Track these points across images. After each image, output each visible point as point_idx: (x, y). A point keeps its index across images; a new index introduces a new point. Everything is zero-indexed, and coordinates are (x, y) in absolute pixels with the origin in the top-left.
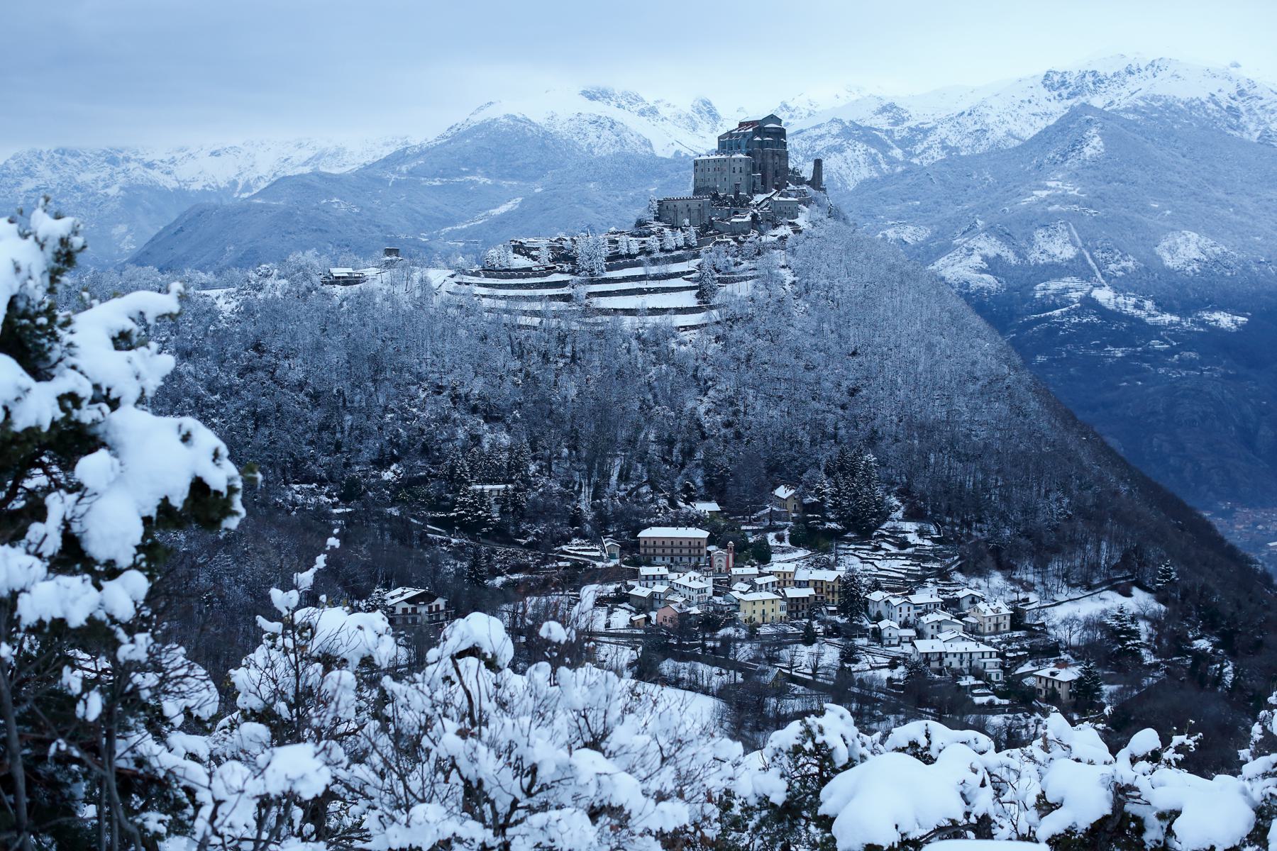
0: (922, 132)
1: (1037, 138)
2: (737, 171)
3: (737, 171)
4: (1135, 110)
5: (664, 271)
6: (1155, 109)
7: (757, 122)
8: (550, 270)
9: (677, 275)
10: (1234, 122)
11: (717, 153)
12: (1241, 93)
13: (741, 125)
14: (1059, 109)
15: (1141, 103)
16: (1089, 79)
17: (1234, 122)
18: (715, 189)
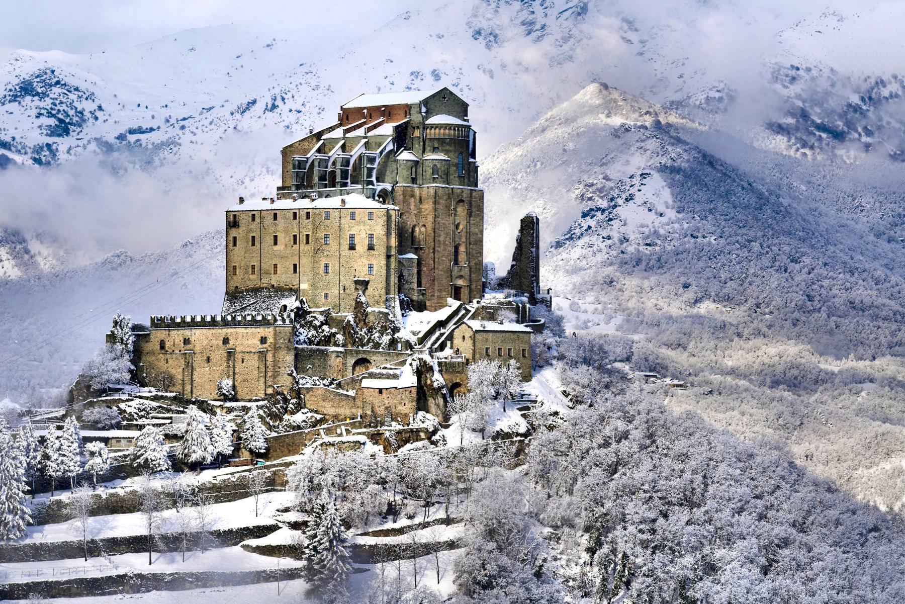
2: (361, 247)
3: (361, 247)
11: (283, 191)
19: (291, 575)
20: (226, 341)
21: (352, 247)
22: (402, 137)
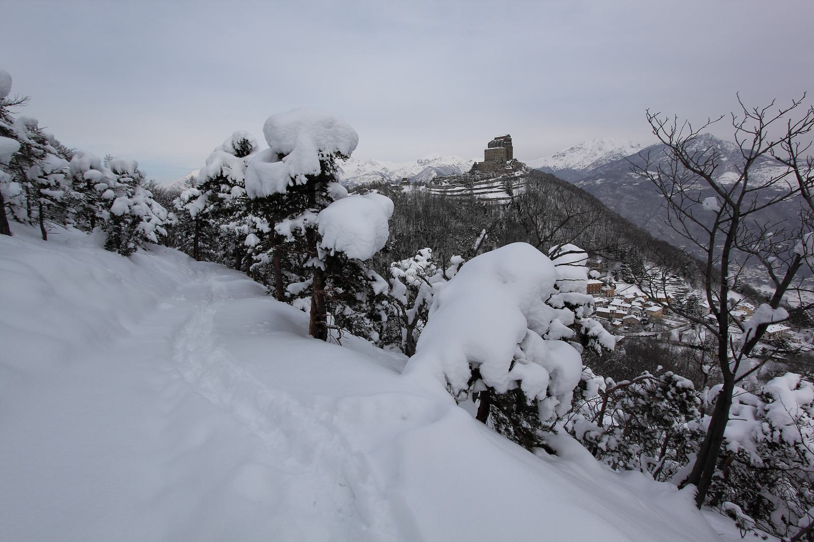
0: (392, 173)
1: (420, 174)
4: (439, 167)
8: (454, 187)
14: (421, 169)
16: (427, 161)
22: (505, 140)
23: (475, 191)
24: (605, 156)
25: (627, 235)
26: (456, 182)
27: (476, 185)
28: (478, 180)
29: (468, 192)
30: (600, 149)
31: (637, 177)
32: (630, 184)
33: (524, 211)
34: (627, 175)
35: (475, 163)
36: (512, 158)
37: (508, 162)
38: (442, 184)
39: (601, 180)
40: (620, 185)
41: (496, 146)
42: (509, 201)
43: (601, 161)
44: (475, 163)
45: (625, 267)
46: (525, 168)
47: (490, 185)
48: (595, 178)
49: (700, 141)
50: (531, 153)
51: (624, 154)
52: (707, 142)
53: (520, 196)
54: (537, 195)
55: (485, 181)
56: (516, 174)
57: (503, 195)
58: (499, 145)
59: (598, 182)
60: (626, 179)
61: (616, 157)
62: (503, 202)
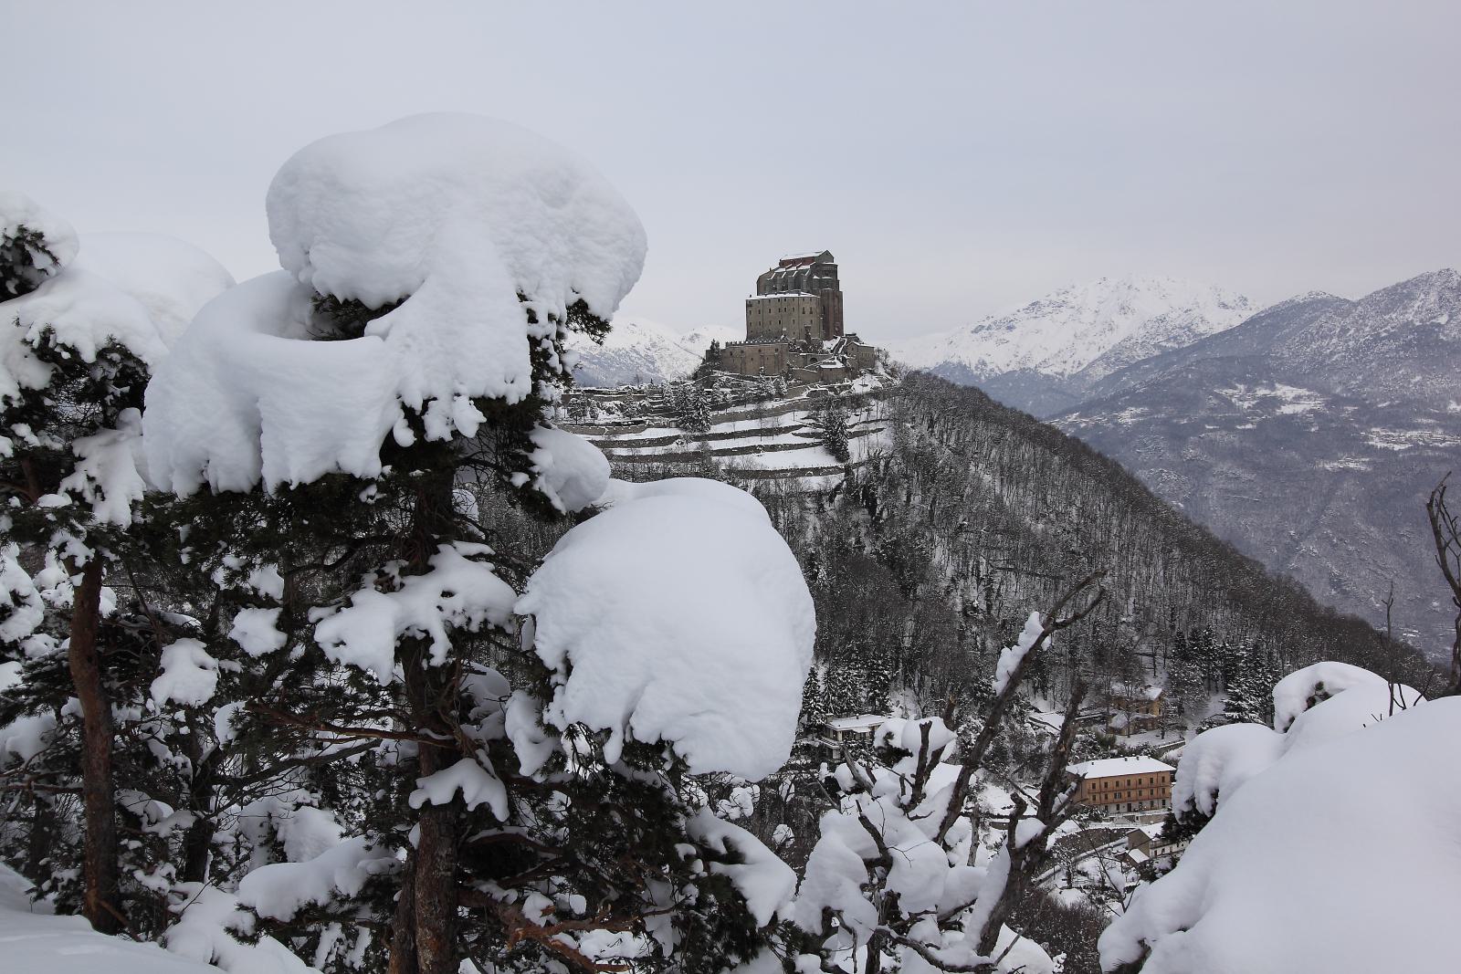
2: (807, 312)
3: (807, 312)
5: (776, 425)
6: (594, 357)
7: (812, 259)
8: (639, 426)
9: (787, 430)
10: (652, 367)
12: (654, 345)
13: (783, 264)
15: (583, 352)
17: (652, 367)
18: (782, 333)
19: (820, 444)
20: (760, 351)
21: (804, 313)
23: (715, 445)
24: (1142, 332)
25: (1237, 600)
26: (645, 410)
27: (718, 421)
28: (726, 406)
29: (693, 446)
30: (1124, 309)
31: (1246, 405)
32: (1228, 425)
33: (891, 516)
34: (1217, 396)
35: (715, 345)
36: (840, 332)
37: (828, 345)
38: (594, 417)
39: (1135, 410)
40: (1197, 428)
41: (785, 289)
42: (836, 480)
43: (1131, 349)
44: (715, 345)
45: (1239, 709)
46: (885, 365)
47: (768, 423)
48: (1113, 405)
49: (1427, 294)
50: (908, 315)
51: (1202, 328)
52: (1448, 294)
53: (873, 461)
54: (932, 459)
55: (751, 407)
56: (859, 386)
57: (817, 457)
58: (796, 284)
59: (1127, 417)
60: (1212, 409)
61: (1175, 338)
62: (815, 483)
